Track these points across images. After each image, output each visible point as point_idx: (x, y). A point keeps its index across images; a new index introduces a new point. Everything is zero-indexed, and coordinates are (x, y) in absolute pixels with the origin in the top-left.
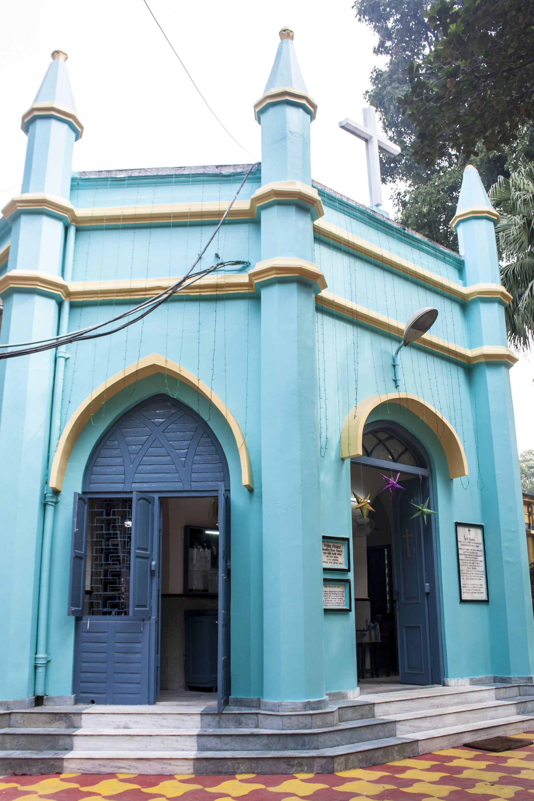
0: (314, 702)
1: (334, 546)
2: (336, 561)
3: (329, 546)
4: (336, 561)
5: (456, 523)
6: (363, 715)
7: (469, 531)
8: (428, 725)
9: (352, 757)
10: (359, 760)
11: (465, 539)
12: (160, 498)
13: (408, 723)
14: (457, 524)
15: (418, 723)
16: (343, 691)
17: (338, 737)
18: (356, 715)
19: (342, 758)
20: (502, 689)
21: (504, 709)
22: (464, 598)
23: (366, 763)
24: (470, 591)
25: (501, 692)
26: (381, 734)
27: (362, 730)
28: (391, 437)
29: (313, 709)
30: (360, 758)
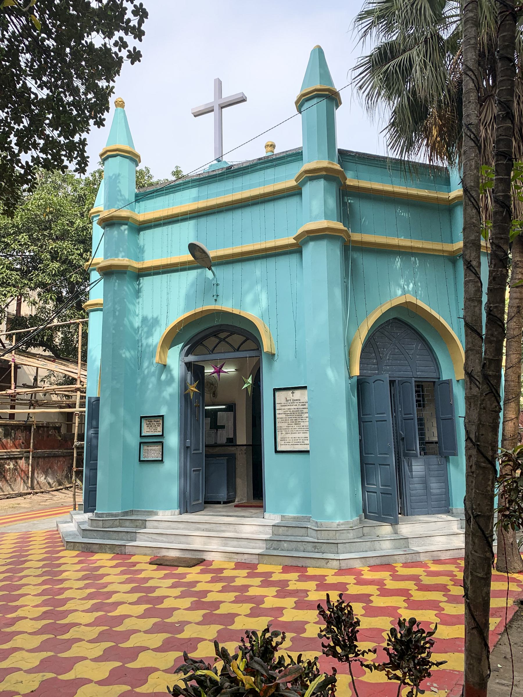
0: (100, 514)
1: (155, 421)
2: (155, 430)
3: (151, 421)
4: (155, 430)
5: (274, 389)
6: (137, 526)
7: (293, 393)
8: (164, 539)
9: (78, 544)
10: (82, 547)
11: (287, 401)
12: (75, 407)
13: (147, 535)
14: (275, 390)
15: (154, 536)
16: (155, 510)
17: (95, 534)
18: (131, 525)
19: (72, 544)
20: (282, 528)
21: (249, 542)
22: (279, 449)
23: (87, 549)
24: (290, 444)
25: (280, 529)
26: (124, 538)
27: (111, 533)
28: (232, 334)
29: (99, 517)
30: (83, 546)
